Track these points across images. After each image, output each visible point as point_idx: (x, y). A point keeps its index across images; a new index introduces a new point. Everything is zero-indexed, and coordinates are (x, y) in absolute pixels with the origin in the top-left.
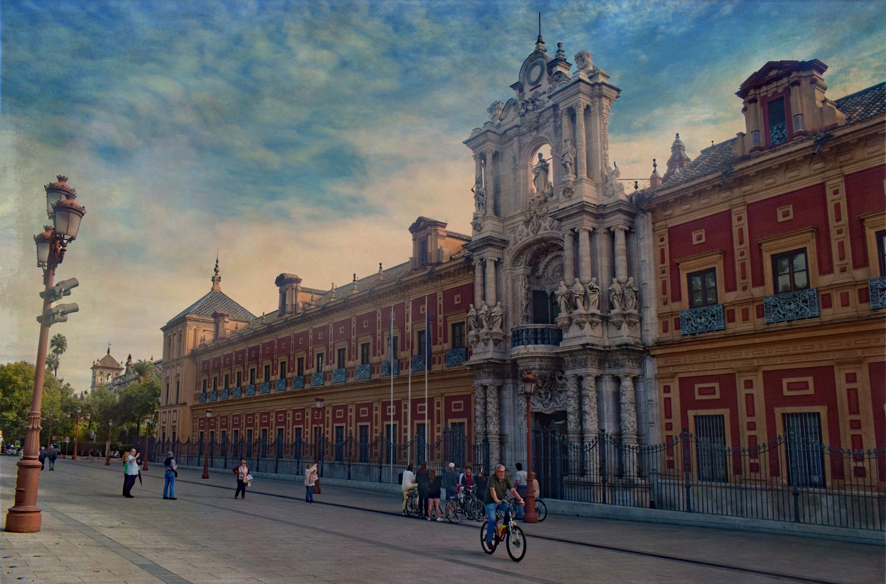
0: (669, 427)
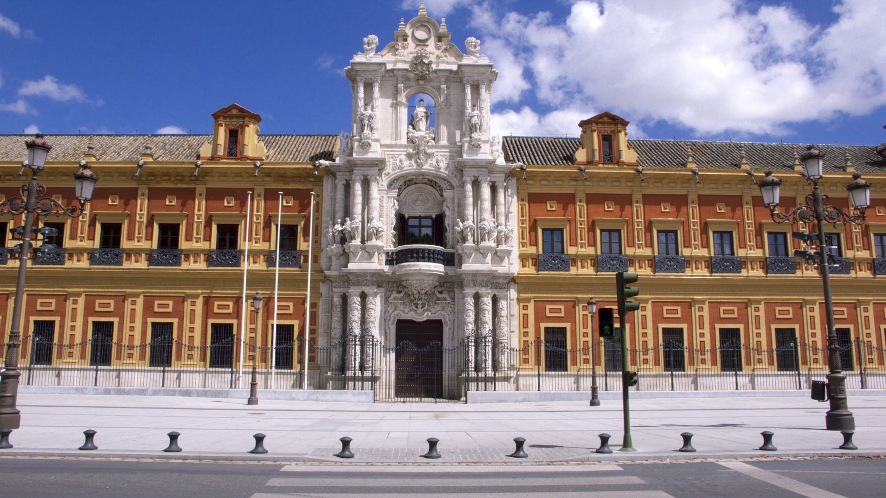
0: (526, 334)
